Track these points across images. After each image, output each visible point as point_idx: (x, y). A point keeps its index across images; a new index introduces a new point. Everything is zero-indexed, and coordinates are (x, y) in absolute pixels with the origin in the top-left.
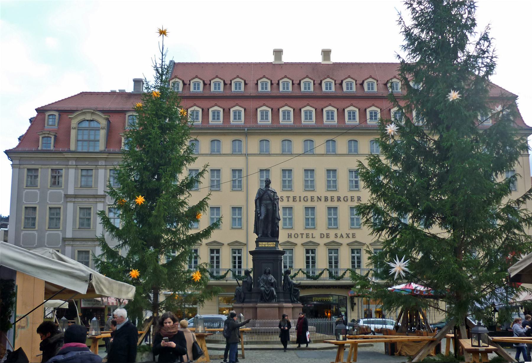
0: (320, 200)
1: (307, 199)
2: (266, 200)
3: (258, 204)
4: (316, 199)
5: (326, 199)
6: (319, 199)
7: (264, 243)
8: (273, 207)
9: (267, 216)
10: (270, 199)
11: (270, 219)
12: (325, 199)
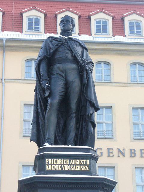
0: (123, 155)
1: (102, 153)
2: (65, 61)
3: (43, 71)
4: (115, 152)
5: (133, 153)
6: (121, 153)
7: (59, 161)
8: (81, 78)
9: (65, 99)
10: (75, 60)
11: (73, 106)
12: (131, 153)
